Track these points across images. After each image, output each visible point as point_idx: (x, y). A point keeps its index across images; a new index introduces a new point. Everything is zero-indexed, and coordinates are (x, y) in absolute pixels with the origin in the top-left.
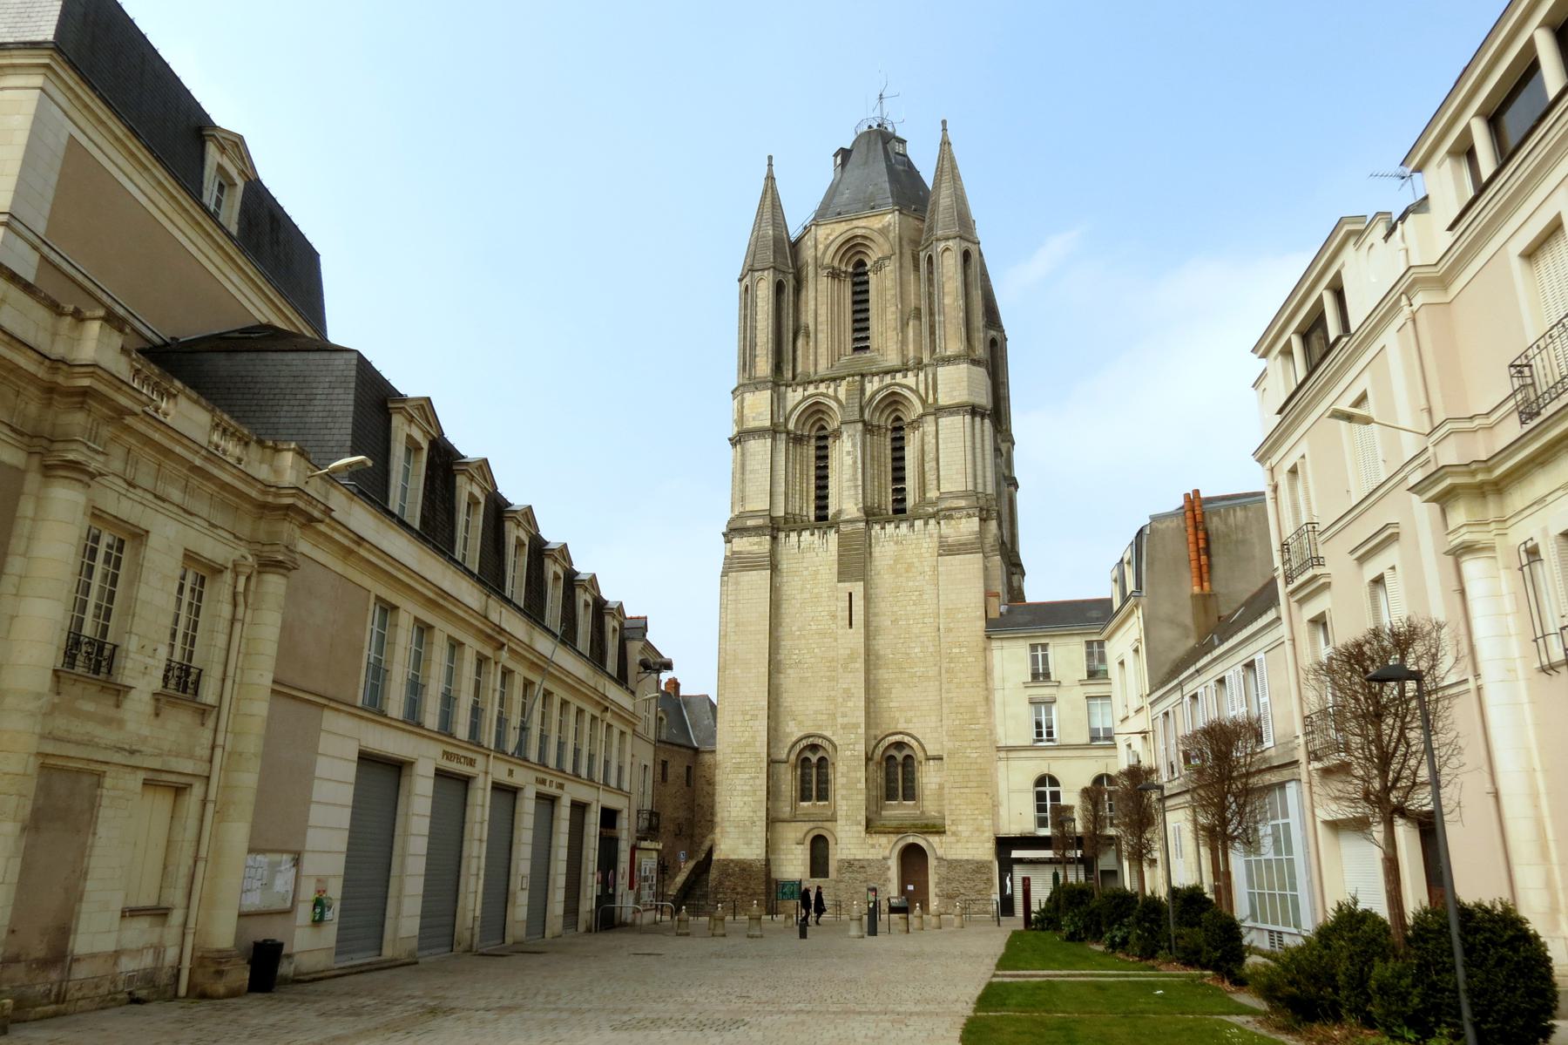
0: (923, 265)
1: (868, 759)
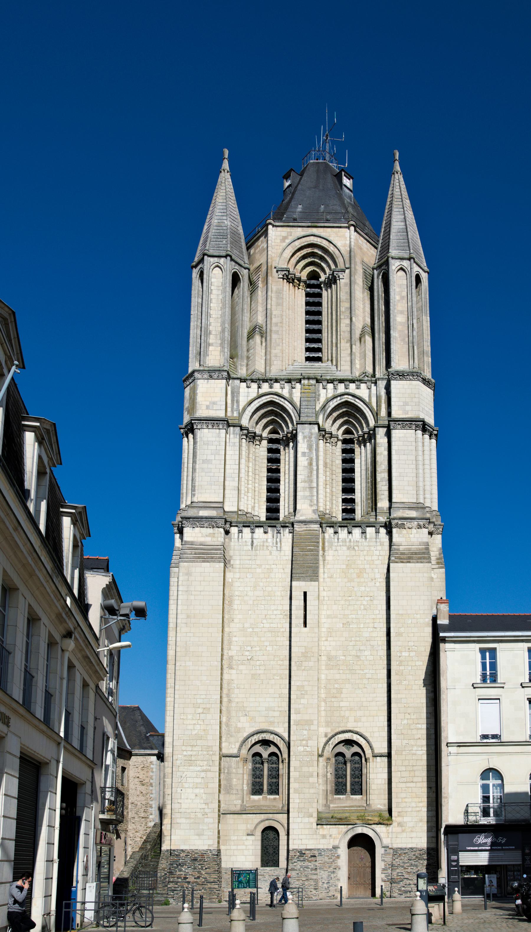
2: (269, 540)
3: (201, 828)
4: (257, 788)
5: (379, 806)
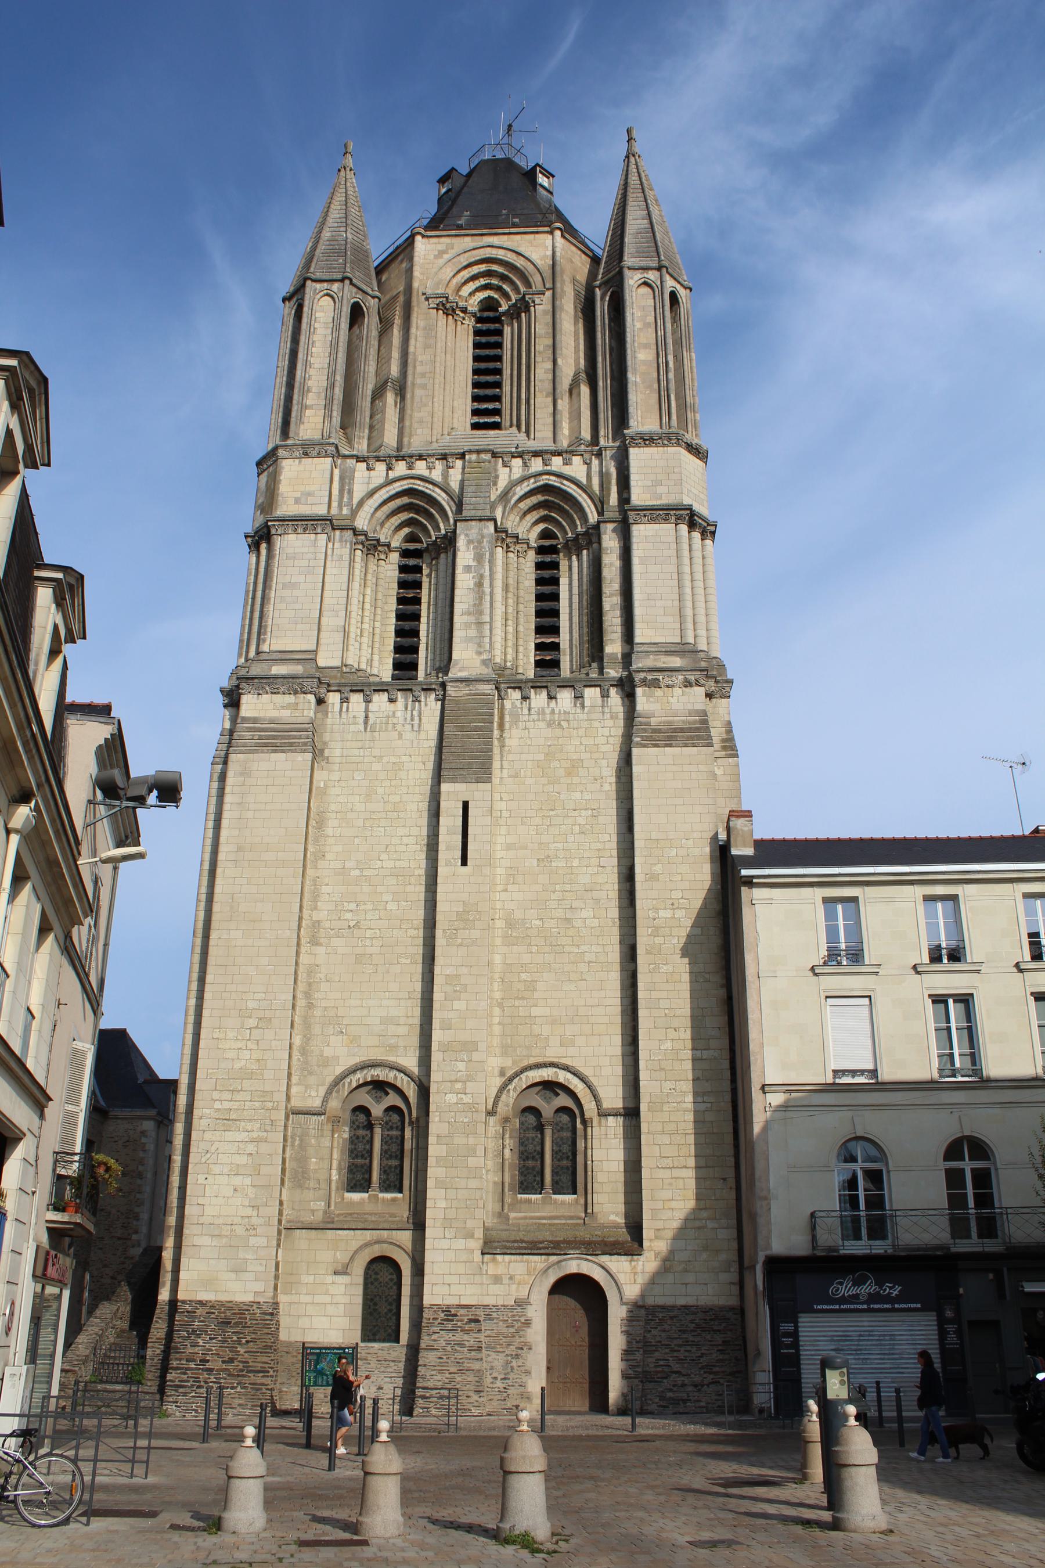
2: (399, 714)
3: (241, 1256)
4: (359, 1177)
5: (612, 1217)
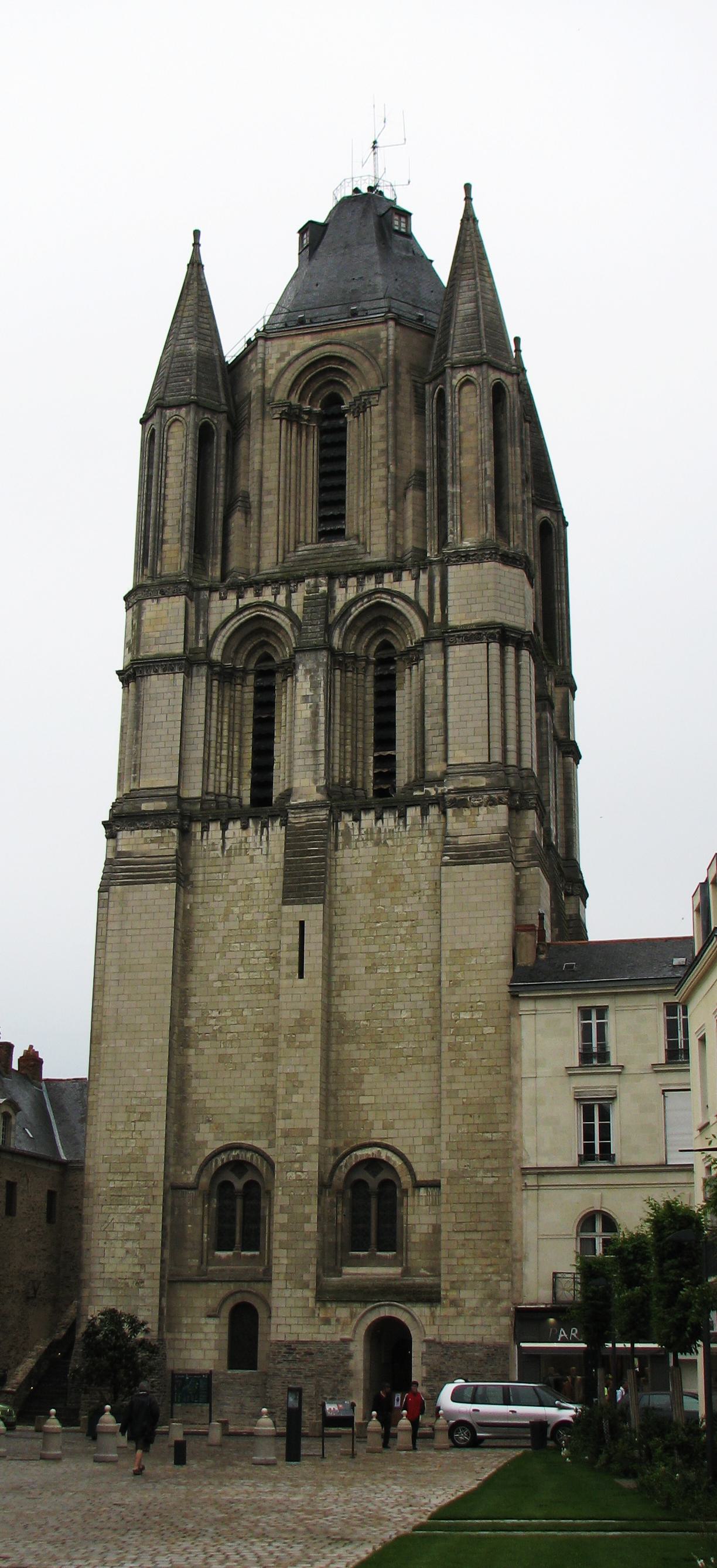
0: (431, 406)
1: (324, 1186)
2: (250, 840)
